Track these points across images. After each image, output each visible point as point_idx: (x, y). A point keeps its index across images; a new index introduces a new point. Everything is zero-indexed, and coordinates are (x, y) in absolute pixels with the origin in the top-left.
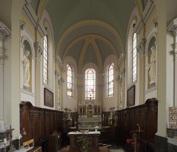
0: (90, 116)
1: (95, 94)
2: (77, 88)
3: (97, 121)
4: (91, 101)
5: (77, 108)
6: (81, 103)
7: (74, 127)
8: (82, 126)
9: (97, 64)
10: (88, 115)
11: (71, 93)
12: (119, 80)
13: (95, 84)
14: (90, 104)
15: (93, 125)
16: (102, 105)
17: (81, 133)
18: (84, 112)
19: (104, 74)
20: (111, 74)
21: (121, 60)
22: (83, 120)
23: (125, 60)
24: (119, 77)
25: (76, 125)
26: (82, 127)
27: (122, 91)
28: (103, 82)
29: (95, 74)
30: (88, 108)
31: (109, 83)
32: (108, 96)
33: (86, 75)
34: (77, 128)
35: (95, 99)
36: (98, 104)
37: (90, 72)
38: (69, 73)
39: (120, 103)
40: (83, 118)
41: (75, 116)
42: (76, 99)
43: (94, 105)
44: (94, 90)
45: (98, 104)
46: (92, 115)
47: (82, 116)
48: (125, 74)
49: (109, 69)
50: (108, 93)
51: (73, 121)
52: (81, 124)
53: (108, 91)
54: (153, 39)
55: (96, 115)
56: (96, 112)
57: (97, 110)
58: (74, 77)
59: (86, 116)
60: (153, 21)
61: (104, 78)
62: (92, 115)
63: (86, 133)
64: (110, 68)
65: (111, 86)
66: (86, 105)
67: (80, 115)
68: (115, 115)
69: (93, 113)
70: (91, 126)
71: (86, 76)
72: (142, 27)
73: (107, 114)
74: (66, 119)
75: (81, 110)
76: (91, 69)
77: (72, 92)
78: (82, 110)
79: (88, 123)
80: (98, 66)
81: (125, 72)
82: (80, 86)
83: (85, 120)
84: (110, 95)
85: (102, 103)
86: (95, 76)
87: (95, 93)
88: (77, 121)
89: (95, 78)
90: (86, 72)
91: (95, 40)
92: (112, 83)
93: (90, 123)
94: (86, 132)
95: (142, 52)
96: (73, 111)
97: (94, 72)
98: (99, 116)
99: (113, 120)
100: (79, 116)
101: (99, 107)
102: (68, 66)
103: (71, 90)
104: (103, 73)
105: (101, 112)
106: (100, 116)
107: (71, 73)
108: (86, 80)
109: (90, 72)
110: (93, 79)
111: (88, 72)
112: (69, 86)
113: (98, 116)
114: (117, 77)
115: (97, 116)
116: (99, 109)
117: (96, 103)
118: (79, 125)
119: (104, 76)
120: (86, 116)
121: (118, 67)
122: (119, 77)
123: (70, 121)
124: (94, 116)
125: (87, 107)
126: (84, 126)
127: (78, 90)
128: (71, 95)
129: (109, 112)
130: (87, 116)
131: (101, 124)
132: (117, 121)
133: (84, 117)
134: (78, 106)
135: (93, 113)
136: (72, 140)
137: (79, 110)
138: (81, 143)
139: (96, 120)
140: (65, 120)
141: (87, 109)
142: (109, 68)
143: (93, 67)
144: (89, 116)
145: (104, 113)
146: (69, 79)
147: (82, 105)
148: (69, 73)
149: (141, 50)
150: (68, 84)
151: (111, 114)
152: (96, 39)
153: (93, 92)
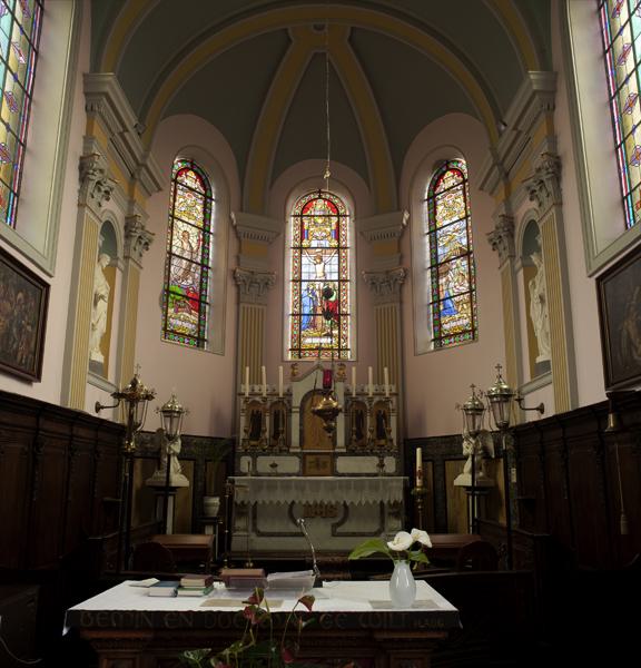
0: (323, 459)
2: (232, 291)
3: (368, 497)
5: (227, 411)
6: (256, 379)
7: (201, 532)
8: (262, 527)
10: (303, 457)
12: (515, 241)
15: (339, 524)
16: (401, 394)
17: (234, 604)
18: (276, 434)
19: (406, 216)
20: (449, 217)
21: (511, 147)
22: (272, 487)
23: (551, 108)
24: (509, 222)
25: (213, 522)
26: (261, 534)
27: (542, 299)
28: (401, 257)
29: (347, 223)
30: (302, 408)
31: (441, 269)
34: (224, 540)
36: (371, 389)
37: (320, 206)
39: (527, 378)
40: (271, 476)
41: (215, 457)
43: (347, 394)
45: (371, 389)
47: (264, 463)
48: (558, 189)
49: (438, 190)
50: (438, 325)
51: (199, 491)
52: (254, 512)
53: (438, 314)
54: (532, 227)
55: (364, 454)
56: (360, 435)
57: (369, 422)
58: (216, 227)
59: (290, 464)
60: (523, 181)
61: (405, 242)
63: (289, 605)
64: (444, 185)
66: (289, 394)
67: (246, 454)
68: (498, 457)
69: (341, 440)
70: (329, 530)
71: (292, 231)
72: (540, 113)
74: (147, 473)
75: (256, 420)
77: (201, 311)
78: (264, 423)
79: (307, 506)
81: (557, 176)
83: (287, 486)
84: (449, 336)
85: (400, 377)
91: (350, 40)
93: (317, 511)
94: (282, 588)
95: (505, 254)
96: (198, 424)
97: (346, 205)
98: (381, 465)
100: (245, 463)
101: (379, 402)
102: (179, 166)
104: (399, 209)
105: (393, 435)
106: (391, 464)
107: (200, 208)
109: (320, 206)
110: (335, 243)
111: (305, 208)
113: (376, 460)
114: (499, 220)
115: (367, 464)
116: (382, 419)
117: (362, 379)
118: (240, 523)
119: (406, 228)
120: (290, 464)
121: (498, 163)
122: (509, 222)
123: (168, 489)
124: (344, 464)
125: (296, 402)
126: (277, 528)
127: (238, 303)
129: (454, 442)
131: (396, 515)
132: (514, 496)
133: (280, 470)
134: (238, 394)
135: (341, 440)
137: (243, 422)
139: (359, 487)
140: (137, 481)
141: (295, 418)
142: (435, 184)
143: (338, 183)
144: (309, 458)
145: (407, 446)
146: (185, 238)
149: (544, 194)
151: (467, 448)
152: (353, 29)
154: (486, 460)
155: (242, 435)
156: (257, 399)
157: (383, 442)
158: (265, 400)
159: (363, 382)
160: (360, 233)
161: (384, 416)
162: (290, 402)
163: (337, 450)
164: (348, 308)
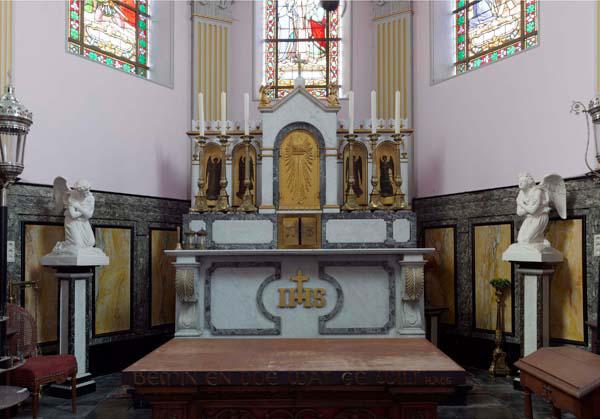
1: (341, 63)
10: (278, 220)
11: (133, 39)
14: (298, 110)
30: (276, 150)
32: (464, 62)
41: (155, 223)
42: (171, 85)
46: (325, 217)
50: (464, 39)
56: (358, 192)
57: (371, 170)
62: (325, 217)
69: (332, 197)
75: (214, 170)
78: (227, 169)
84: (481, 55)
101: (386, 144)
105: (404, 189)
113: (382, 223)
116: (387, 167)
117: (363, 109)
125: (268, 141)
130: (268, 225)
135: (332, 197)
137: (197, 173)
140: (34, 260)
147: (224, 126)
155: (196, 191)
156: (216, 140)
157: (389, 200)
158: (224, 139)
159: (361, 113)
161: (391, 164)
162: (259, 144)
163: (326, 211)
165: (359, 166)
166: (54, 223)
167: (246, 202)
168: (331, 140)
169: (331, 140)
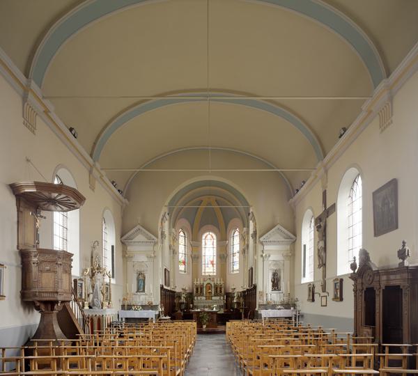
1: (215, 268)
4: (210, 278)
6: (197, 281)
9: (218, 227)
13: (215, 254)
14: (208, 281)
16: (225, 284)
29: (215, 241)
33: (203, 241)
35: (215, 274)
36: (219, 283)
37: (209, 237)
38: (182, 240)
41: (190, 296)
44: (215, 262)
47: (199, 298)
59: (204, 298)
65: (236, 258)
71: (203, 243)
73: (229, 296)
75: (197, 289)
76: (211, 233)
78: (199, 290)
80: (219, 229)
82: (195, 257)
85: (225, 280)
86: (215, 244)
87: (215, 266)
88: (192, 303)
89: (215, 246)
90: (204, 237)
92: (237, 255)
99: (238, 303)
100: (196, 298)
103: (184, 263)
106: (222, 298)
108: (203, 249)
109: (209, 237)
112: (181, 257)
115: (218, 298)
116: (221, 288)
117: (217, 280)
120: (204, 298)
124: (213, 298)
125: (205, 285)
128: (183, 269)
134: (193, 284)
136: (194, 315)
138: (203, 317)
148: (182, 240)
150: (180, 255)
153: (213, 264)
154: (238, 298)
159: (218, 282)
160: (217, 244)
164: (215, 262)
165: (217, 288)
166: (180, 297)
167: (201, 294)
168: (213, 285)
169: (213, 285)
